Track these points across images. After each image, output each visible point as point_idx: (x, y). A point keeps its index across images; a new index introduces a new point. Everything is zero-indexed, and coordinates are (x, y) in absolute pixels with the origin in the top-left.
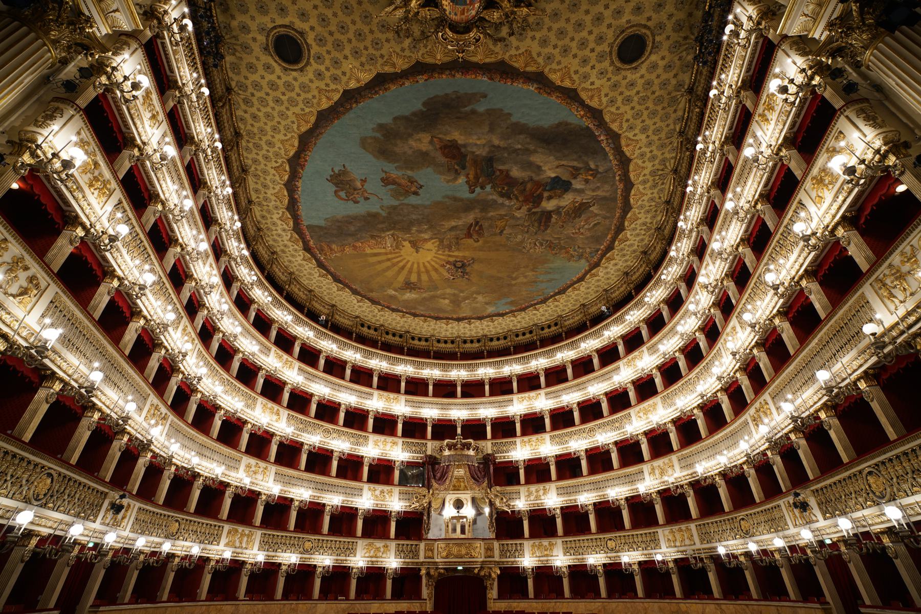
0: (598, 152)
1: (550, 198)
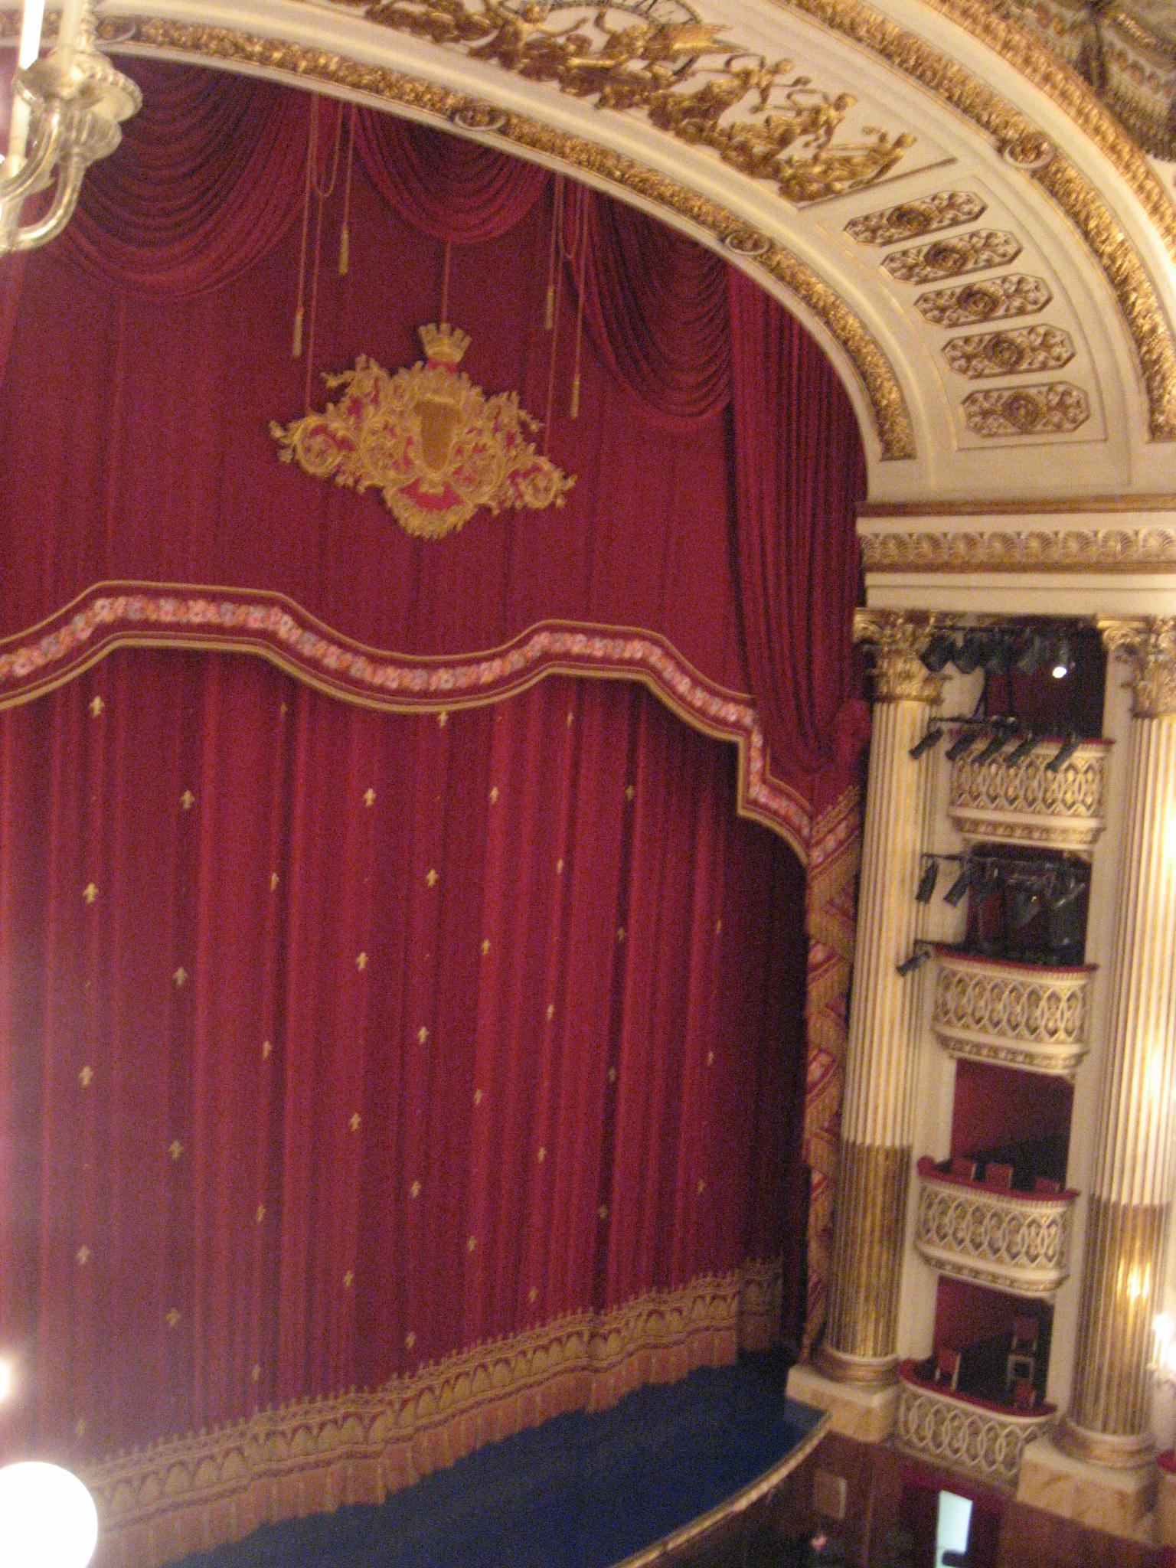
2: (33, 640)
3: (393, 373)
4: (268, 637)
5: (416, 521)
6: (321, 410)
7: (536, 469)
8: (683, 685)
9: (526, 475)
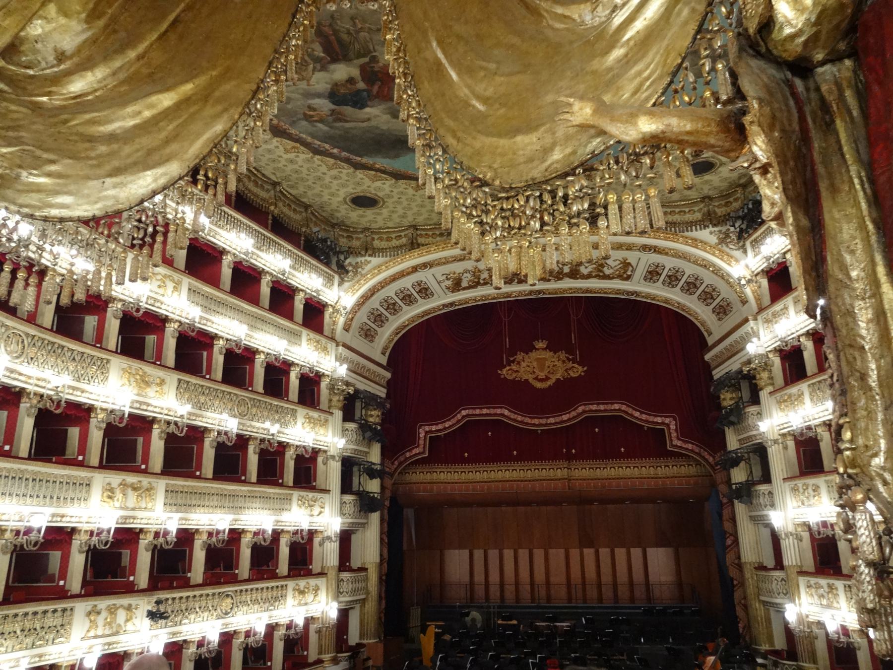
0: (327, 139)
1: (351, 80)
2: (449, 420)
3: (527, 354)
4: (503, 415)
5: (539, 385)
6: (510, 365)
7: (573, 367)
8: (637, 414)
9: (570, 369)
